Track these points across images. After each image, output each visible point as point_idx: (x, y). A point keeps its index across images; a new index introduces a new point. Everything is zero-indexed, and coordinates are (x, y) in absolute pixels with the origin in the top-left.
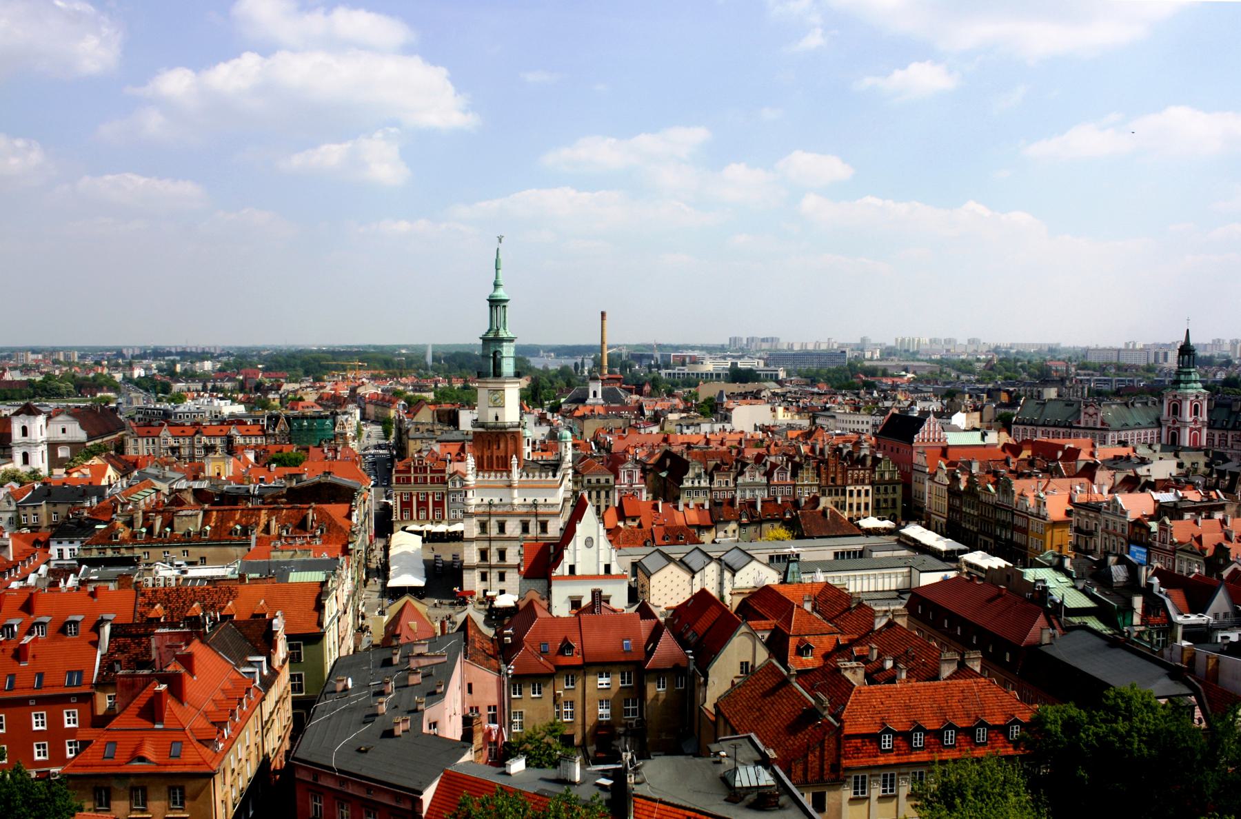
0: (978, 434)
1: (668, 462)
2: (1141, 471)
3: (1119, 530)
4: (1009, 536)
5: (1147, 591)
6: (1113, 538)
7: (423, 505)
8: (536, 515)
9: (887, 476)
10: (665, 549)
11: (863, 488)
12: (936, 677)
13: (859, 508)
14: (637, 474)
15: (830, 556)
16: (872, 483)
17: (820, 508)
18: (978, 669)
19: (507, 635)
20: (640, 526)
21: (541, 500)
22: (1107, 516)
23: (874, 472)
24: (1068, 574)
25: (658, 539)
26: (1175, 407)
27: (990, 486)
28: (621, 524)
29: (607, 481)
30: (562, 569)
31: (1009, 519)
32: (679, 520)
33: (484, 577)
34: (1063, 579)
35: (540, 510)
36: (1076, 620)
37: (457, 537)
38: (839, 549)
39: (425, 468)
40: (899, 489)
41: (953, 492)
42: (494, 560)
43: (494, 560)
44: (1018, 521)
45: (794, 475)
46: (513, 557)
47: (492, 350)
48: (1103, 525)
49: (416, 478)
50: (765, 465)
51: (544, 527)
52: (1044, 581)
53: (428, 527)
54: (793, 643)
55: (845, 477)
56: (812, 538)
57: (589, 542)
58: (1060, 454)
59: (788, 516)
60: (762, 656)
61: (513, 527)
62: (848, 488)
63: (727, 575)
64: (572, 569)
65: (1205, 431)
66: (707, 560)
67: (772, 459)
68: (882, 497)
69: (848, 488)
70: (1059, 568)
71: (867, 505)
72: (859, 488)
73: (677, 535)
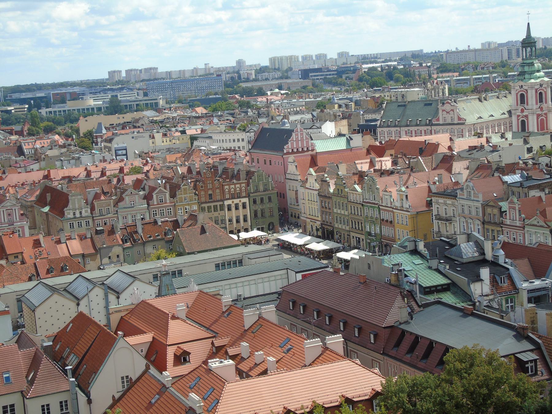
0: (343, 140)
3: (474, 213)
4: (378, 231)
5: (494, 264)
6: (470, 221)
10: (51, 281)
13: (238, 221)
14: (17, 212)
16: (248, 196)
22: (462, 202)
23: (248, 184)
24: (422, 256)
25: (42, 272)
26: (522, 96)
27: (357, 187)
32: (62, 250)
34: (418, 261)
36: (431, 298)
41: (324, 196)
44: (386, 216)
45: (173, 195)
48: (460, 211)
54: (170, 353)
56: (193, 253)
63: (112, 297)
66: (90, 286)
67: (151, 183)
68: (259, 207)
69: (227, 203)
72: (236, 201)
73: (61, 267)
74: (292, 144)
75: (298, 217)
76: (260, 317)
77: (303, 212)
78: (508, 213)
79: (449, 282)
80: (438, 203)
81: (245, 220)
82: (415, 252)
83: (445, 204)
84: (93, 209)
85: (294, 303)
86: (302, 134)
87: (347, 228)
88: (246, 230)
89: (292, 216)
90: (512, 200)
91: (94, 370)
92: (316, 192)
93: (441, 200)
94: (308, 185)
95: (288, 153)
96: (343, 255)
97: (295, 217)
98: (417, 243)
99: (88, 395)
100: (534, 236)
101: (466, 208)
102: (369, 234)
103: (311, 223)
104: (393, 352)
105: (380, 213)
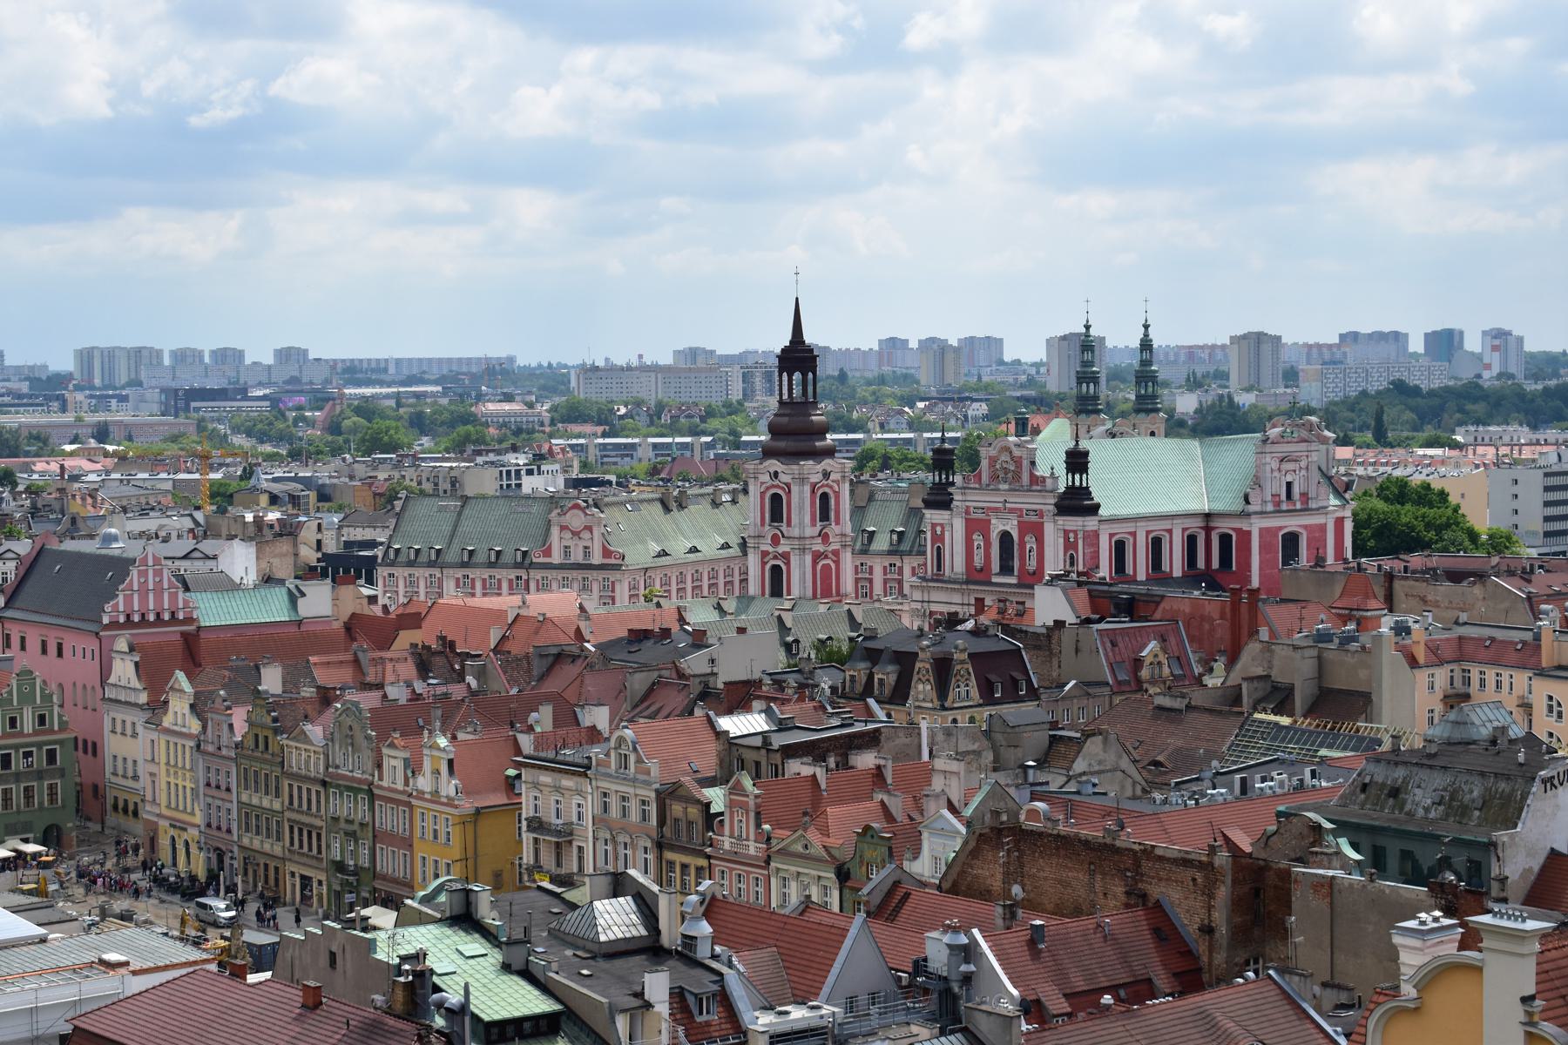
26: (776, 499)
31: (361, 812)
34: (474, 945)
52: (420, 956)
70: (464, 919)
74: (128, 600)
75: (136, 814)
77: (149, 797)
78: (727, 818)
79: (557, 1007)
80: (536, 785)
83: (558, 789)
86: (159, 573)
87: (278, 850)
89: (115, 807)
90: (738, 782)
92: (192, 744)
93: (546, 778)
94: (167, 721)
95: (114, 625)
97: (125, 811)
98: (472, 896)
100: (793, 885)
101: (614, 803)
103: (172, 832)
105: (372, 809)
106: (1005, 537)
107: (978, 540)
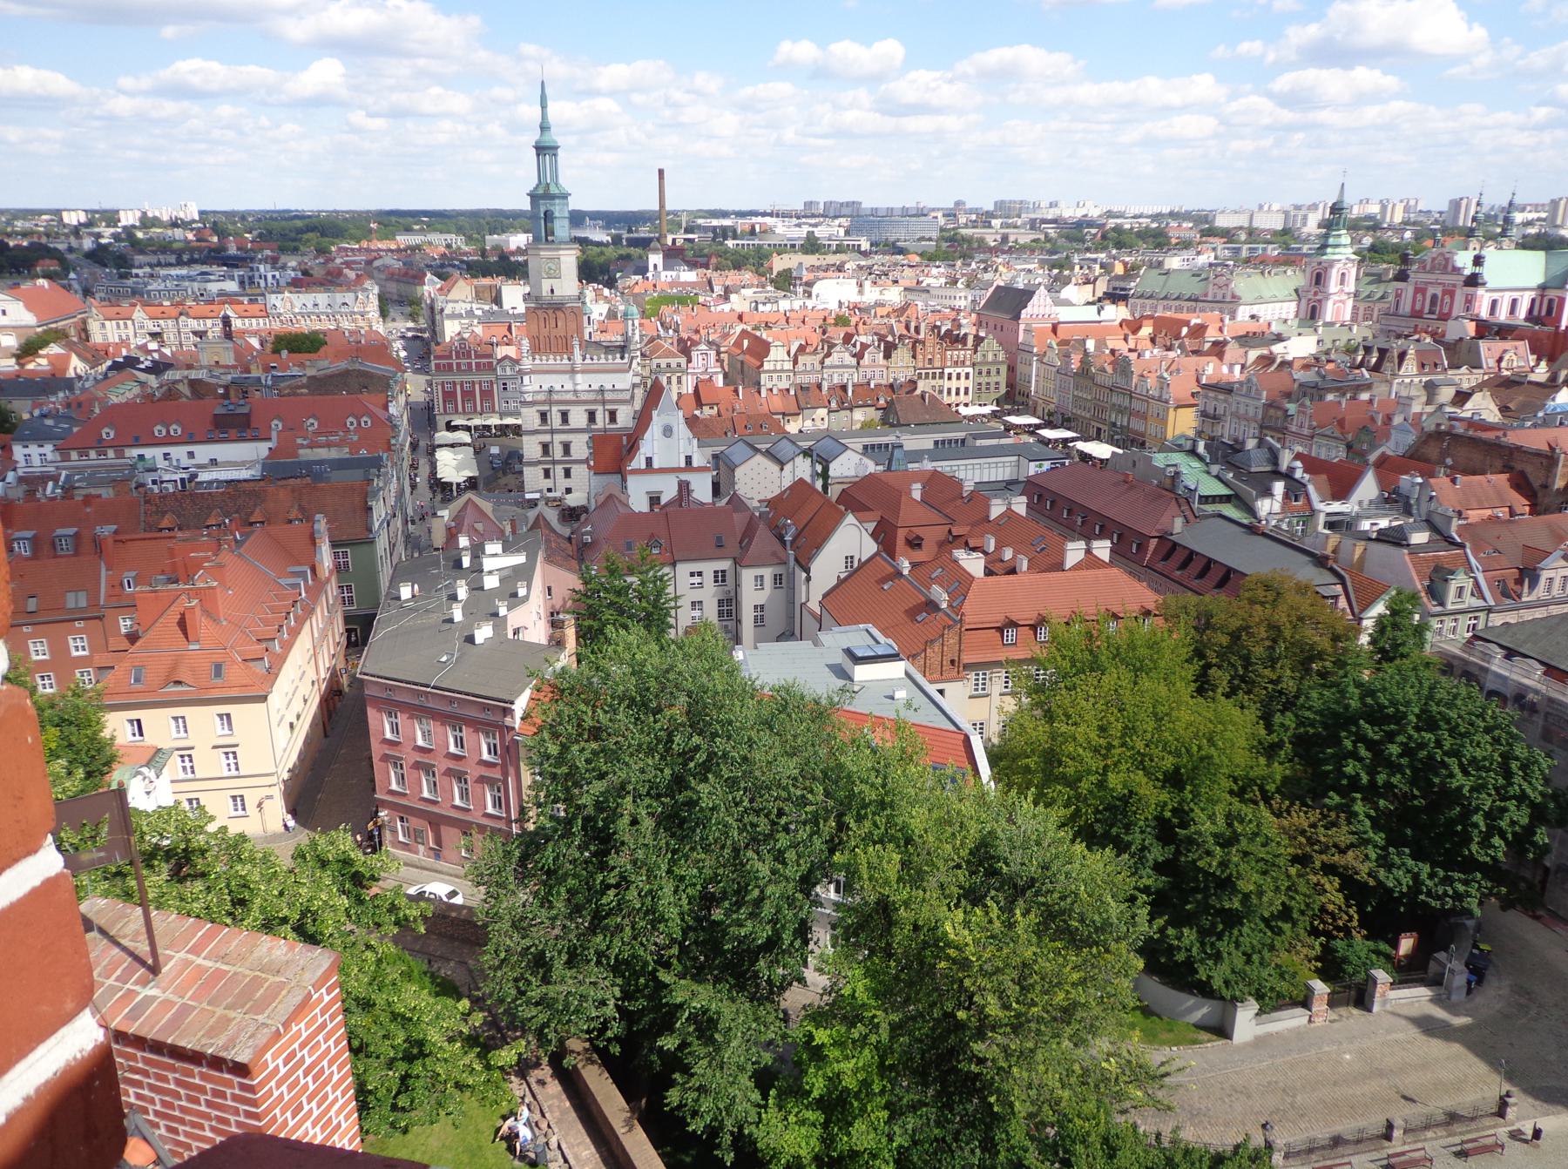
0: (1094, 308)
1: (746, 343)
2: (1277, 348)
5: (1288, 476)
7: (468, 395)
8: (604, 402)
9: (990, 358)
11: (962, 371)
12: (1059, 566)
13: (958, 393)
15: (931, 446)
16: (974, 365)
17: (918, 392)
18: (1107, 559)
19: (587, 533)
20: (719, 415)
21: (608, 386)
24: (1200, 458)
26: (1319, 276)
28: (697, 412)
29: (679, 365)
30: (639, 462)
31: (1127, 403)
33: (547, 474)
34: (1196, 464)
35: (608, 396)
36: (1210, 508)
37: (517, 430)
38: (939, 437)
39: (469, 352)
40: (1004, 369)
42: (558, 453)
43: (558, 453)
44: (1136, 405)
45: (887, 356)
46: (580, 448)
47: (543, 209)
49: (459, 365)
50: (854, 346)
51: (613, 416)
53: (477, 421)
54: (901, 534)
55: (943, 359)
57: (668, 431)
58: (1185, 330)
59: (882, 402)
60: (870, 547)
61: (578, 418)
62: (947, 371)
64: (649, 461)
65: (1350, 303)
67: (863, 339)
68: (984, 380)
71: (967, 389)
72: (959, 370)
76: (1009, 509)
81: (966, 393)
82: (1193, 452)
84: (795, 362)
85: (1040, 496)
88: (966, 405)
91: (819, 546)
96: (1080, 445)
99: (807, 571)
101: (1242, 407)
102: (1114, 425)
104: (1160, 566)
106: (1434, 297)
107: (1419, 296)
